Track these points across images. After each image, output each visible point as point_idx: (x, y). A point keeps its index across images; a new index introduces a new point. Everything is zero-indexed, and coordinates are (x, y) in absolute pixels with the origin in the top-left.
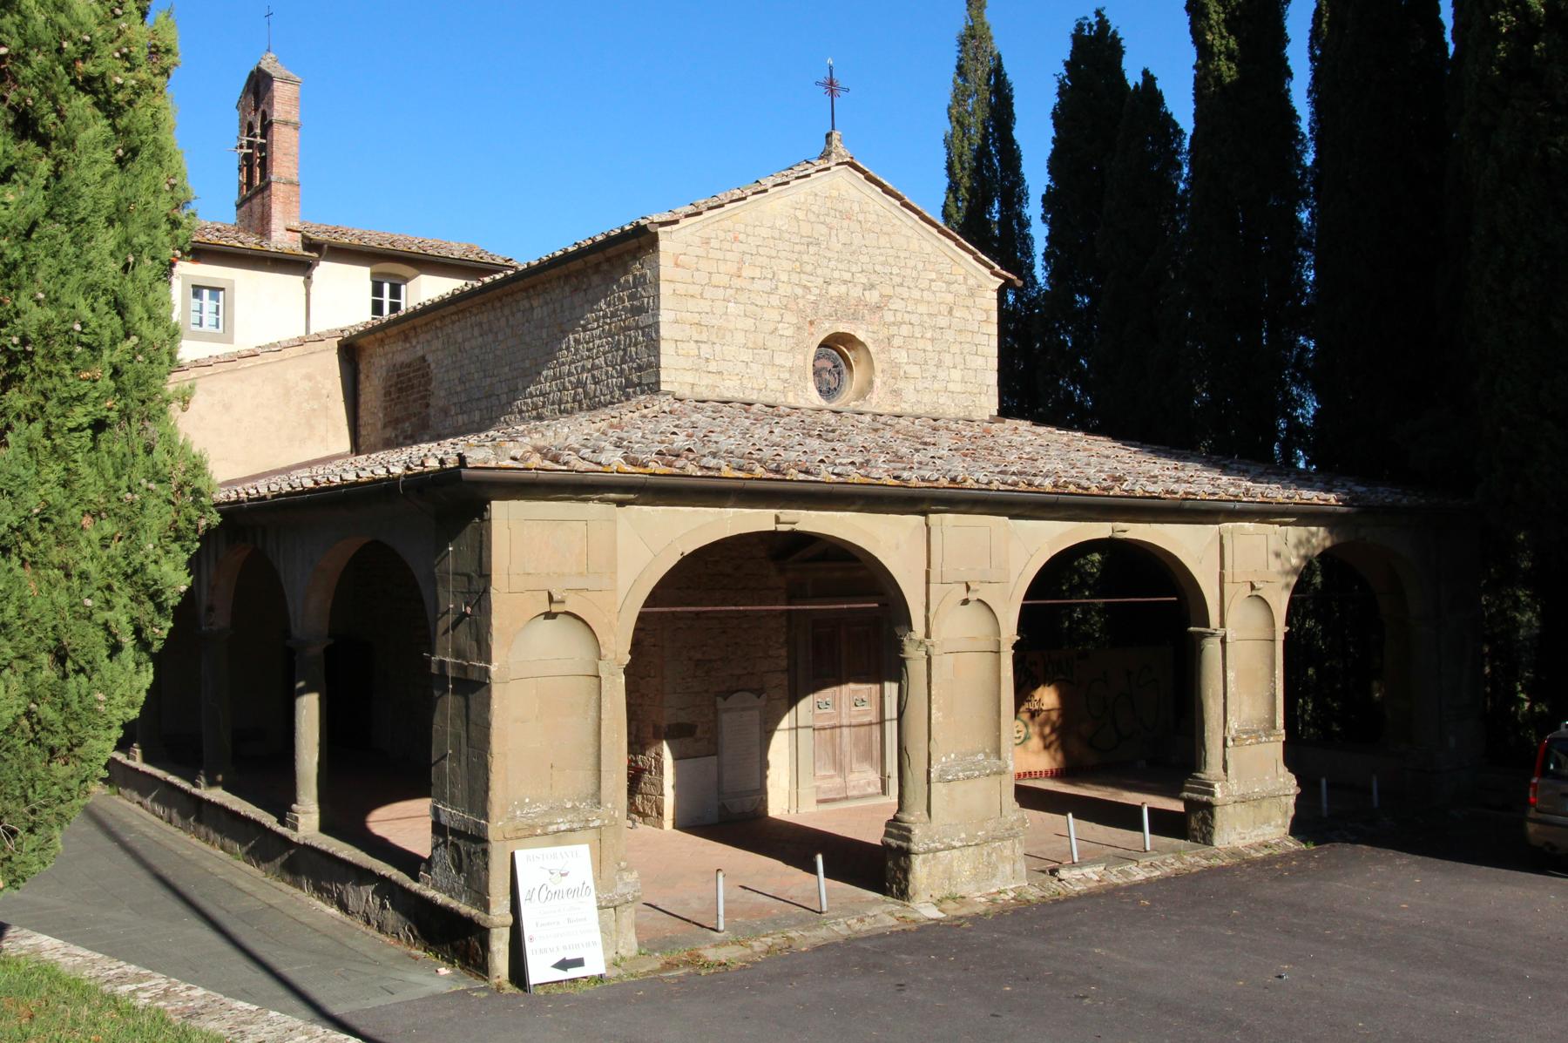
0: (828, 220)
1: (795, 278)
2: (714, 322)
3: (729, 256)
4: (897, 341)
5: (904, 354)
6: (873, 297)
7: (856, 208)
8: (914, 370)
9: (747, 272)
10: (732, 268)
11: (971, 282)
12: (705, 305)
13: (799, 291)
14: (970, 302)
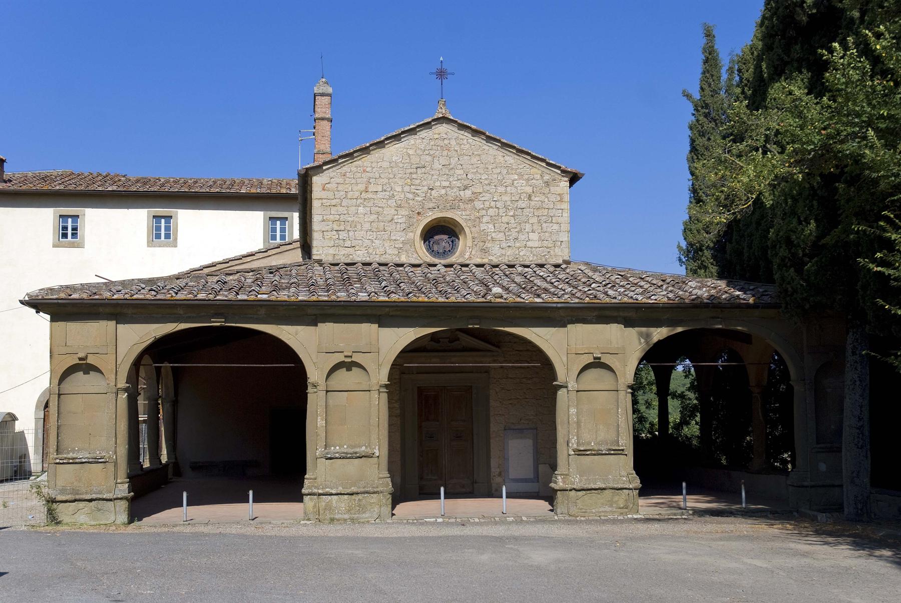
0: (432, 152)
1: (407, 188)
2: (349, 219)
3: (359, 181)
4: (485, 219)
5: (491, 226)
6: (468, 193)
7: (453, 142)
8: (500, 236)
9: (372, 188)
10: (361, 187)
11: (547, 177)
12: (341, 210)
13: (411, 196)
14: (547, 190)
